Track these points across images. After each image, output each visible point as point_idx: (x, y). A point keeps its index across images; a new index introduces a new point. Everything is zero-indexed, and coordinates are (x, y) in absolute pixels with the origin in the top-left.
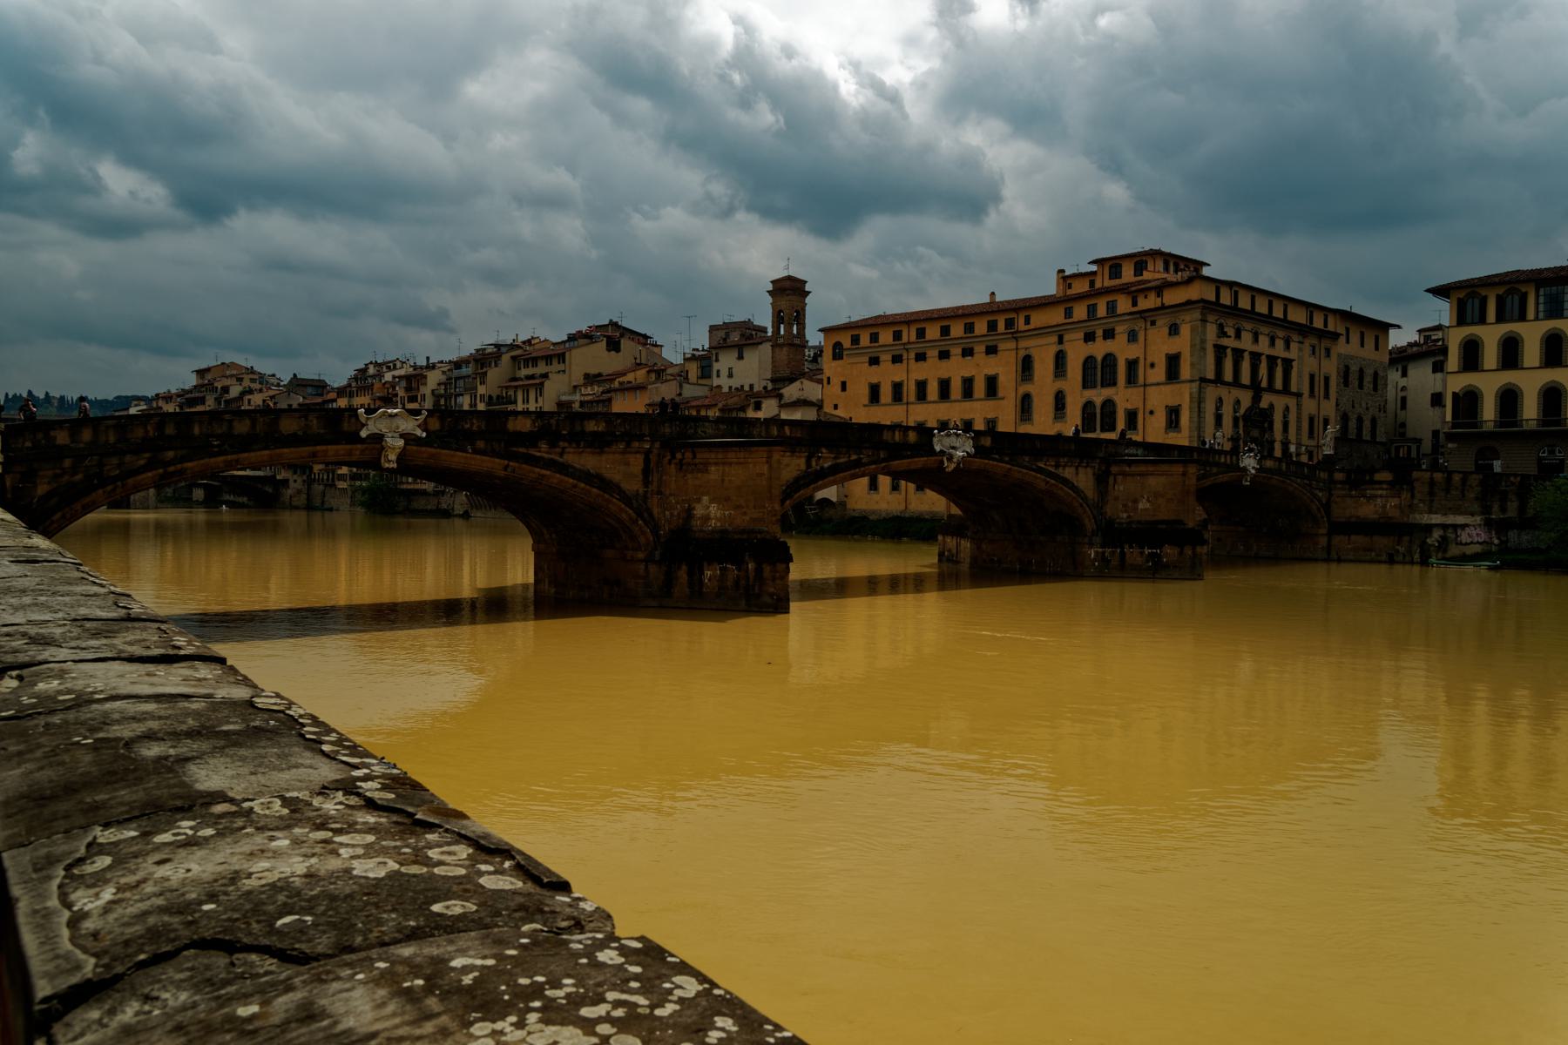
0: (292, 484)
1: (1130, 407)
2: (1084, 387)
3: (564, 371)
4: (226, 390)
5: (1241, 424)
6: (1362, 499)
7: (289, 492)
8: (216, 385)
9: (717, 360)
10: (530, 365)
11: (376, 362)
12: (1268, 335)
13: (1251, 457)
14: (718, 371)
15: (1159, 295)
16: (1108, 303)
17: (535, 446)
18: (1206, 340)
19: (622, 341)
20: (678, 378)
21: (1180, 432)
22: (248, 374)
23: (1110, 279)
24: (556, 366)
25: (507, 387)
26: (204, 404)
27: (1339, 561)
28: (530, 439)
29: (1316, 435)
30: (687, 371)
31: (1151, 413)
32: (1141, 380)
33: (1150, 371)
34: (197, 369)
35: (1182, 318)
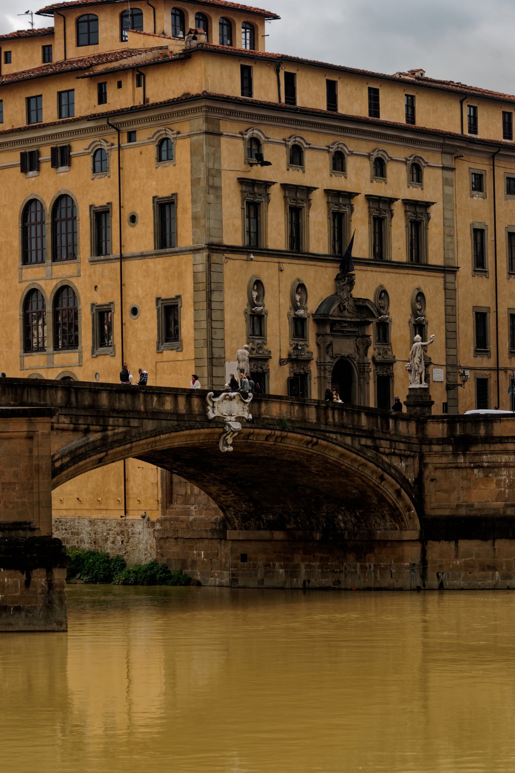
1: (100, 301)
2: (26, 260)
5: (311, 329)
6: (476, 471)
12: (369, 156)
13: (231, 399)
15: (140, 81)
16: (60, 94)
18: (219, 172)
21: (179, 349)
23: (78, 45)
27: (441, 588)
29: (492, 347)
31: (135, 311)
32: (115, 252)
33: (129, 230)
35: (176, 127)
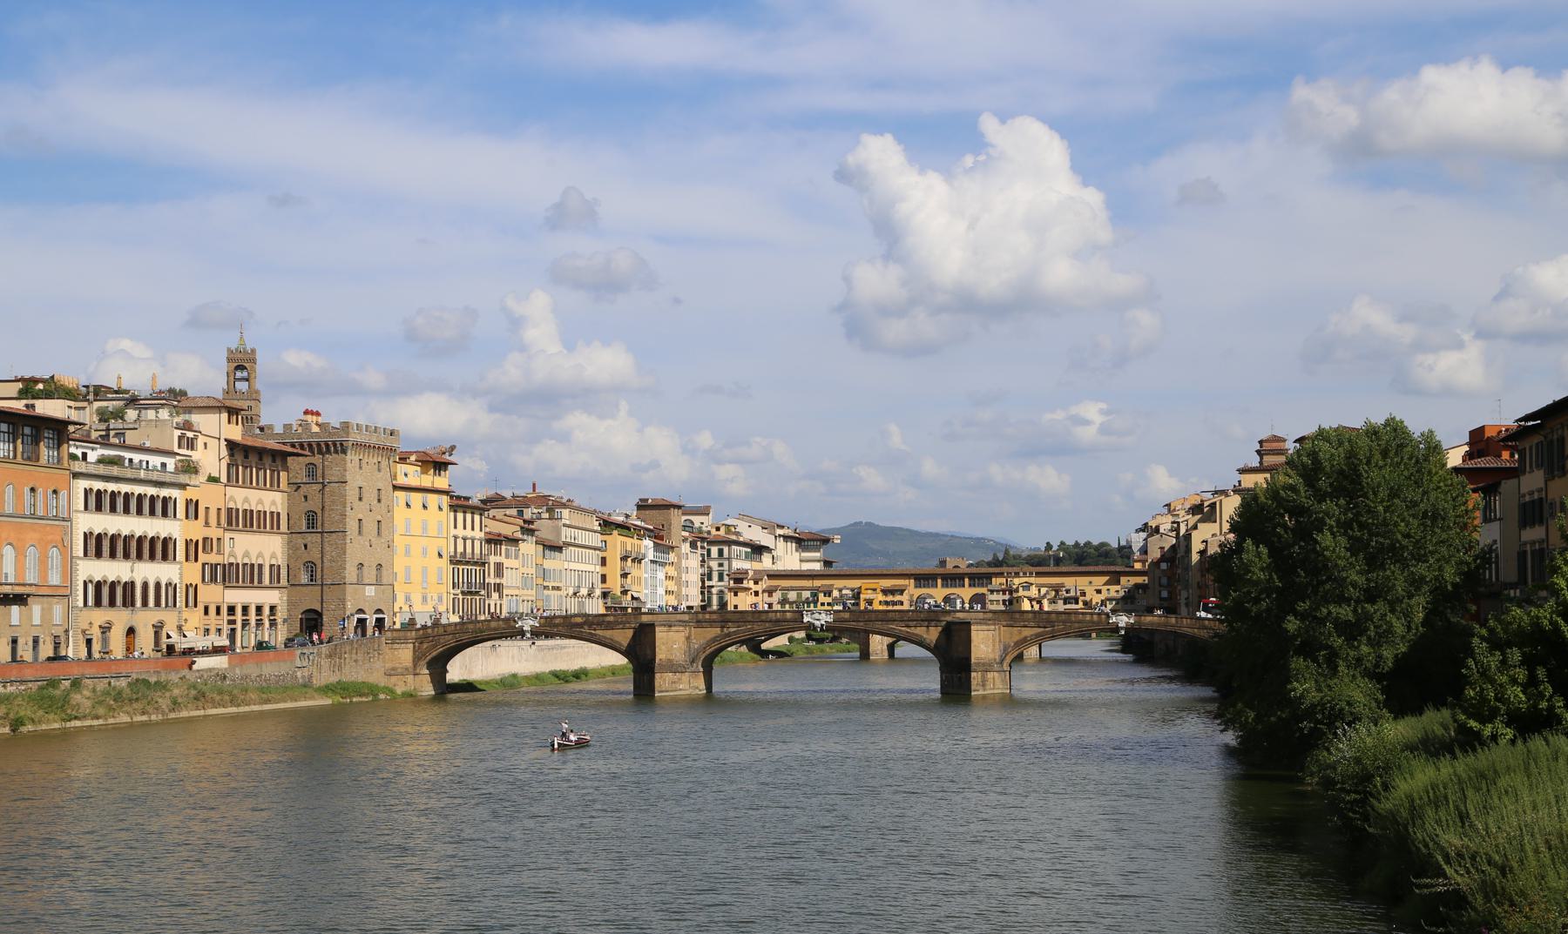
3: (1215, 522)
8: (1150, 524)
17: (582, 628)
28: (580, 625)
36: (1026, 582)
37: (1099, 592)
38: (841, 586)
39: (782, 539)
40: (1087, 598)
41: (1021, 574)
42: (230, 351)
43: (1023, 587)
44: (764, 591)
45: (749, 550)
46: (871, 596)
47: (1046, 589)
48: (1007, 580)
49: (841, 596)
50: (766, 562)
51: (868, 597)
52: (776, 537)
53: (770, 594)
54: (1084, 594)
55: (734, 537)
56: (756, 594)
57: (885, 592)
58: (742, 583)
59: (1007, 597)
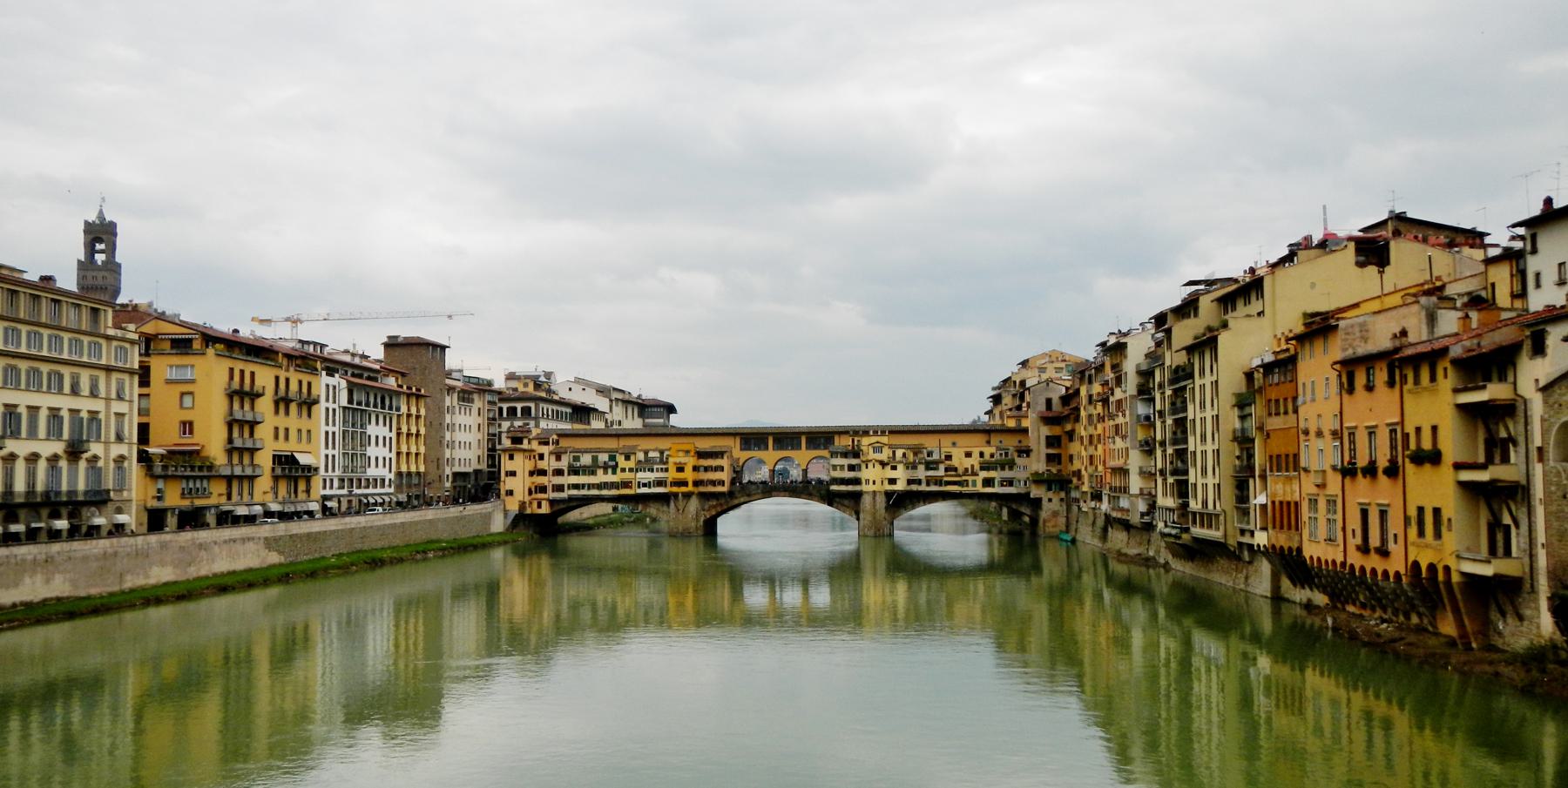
0: (1045, 503)
4: (1023, 383)
7: (1044, 514)
8: (1013, 379)
9: (1534, 251)
10: (1230, 311)
11: (1120, 331)
14: (1538, 275)
19: (1393, 244)
20: (1423, 300)
22: (1053, 362)
24: (1256, 306)
25: (1190, 350)
26: (1001, 403)
30: (1493, 285)
34: (1022, 360)
36: (878, 442)
37: (968, 455)
38: (648, 448)
39: (620, 403)
40: (955, 462)
41: (871, 433)
42: (87, 223)
43: (874, 448)
44: (551, 453)
45: (569, 410)
46: (683, 460)
47: (904, 450)
48: (853, 441)
49: (647, 460)
50: (597, 424)
51: (678, 460)
52: (611, 401)
53: (558, 458)
54: (949, 457)
55: (543, 394)
56: (541, 457)
57: (701, 455)
58: (522, 443)
59: (854, 462)
